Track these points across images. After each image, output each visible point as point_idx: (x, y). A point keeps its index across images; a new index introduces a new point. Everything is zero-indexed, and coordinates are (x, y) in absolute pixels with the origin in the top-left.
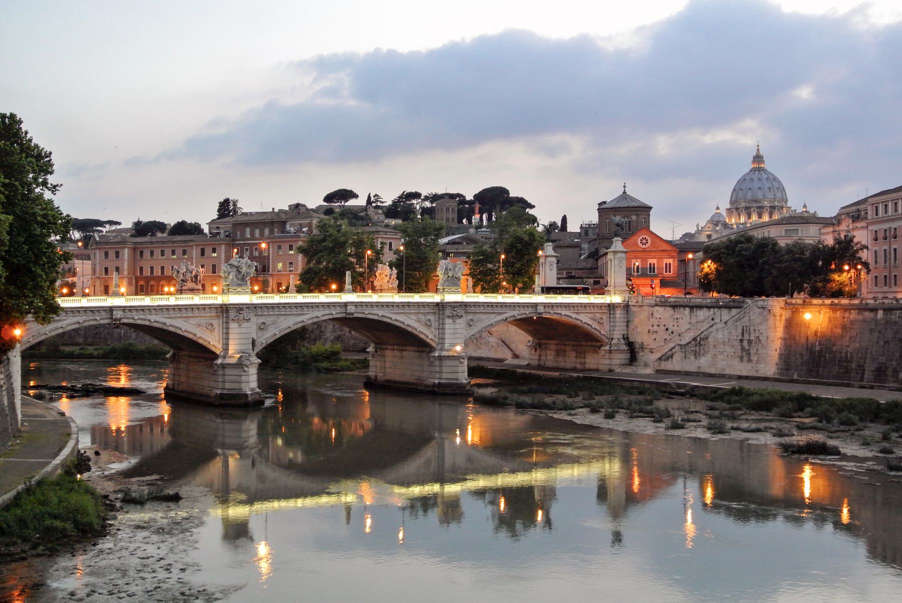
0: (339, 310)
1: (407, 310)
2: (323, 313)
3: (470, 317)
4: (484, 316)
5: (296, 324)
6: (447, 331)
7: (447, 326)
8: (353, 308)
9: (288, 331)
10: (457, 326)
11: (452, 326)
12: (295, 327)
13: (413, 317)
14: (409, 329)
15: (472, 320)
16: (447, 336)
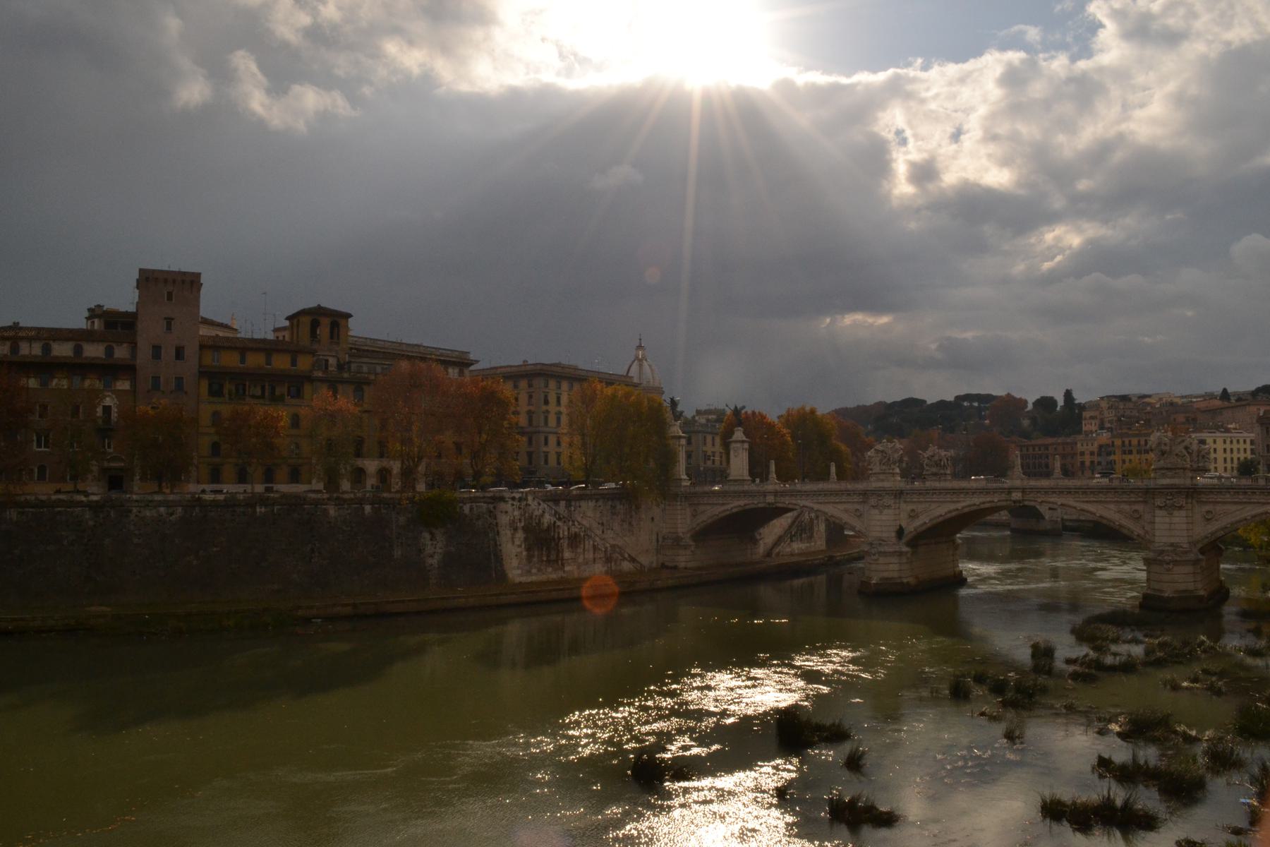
0: (1004, 496)
1: (1102, 497)
2: (981, 500)
3: (1207, 508)
4: (1234, 508)
5: (950, 512)
6: (1157, 526)
7: (1157, 520)
8: (1020, 495)
9: (941, 519)
10: (1176, 520)
11: (1167, 520)
12: (949, 515)
13: (1112, 506)
14: (1105, 522)
15: (1208, 512)
16: (1157, 533)
